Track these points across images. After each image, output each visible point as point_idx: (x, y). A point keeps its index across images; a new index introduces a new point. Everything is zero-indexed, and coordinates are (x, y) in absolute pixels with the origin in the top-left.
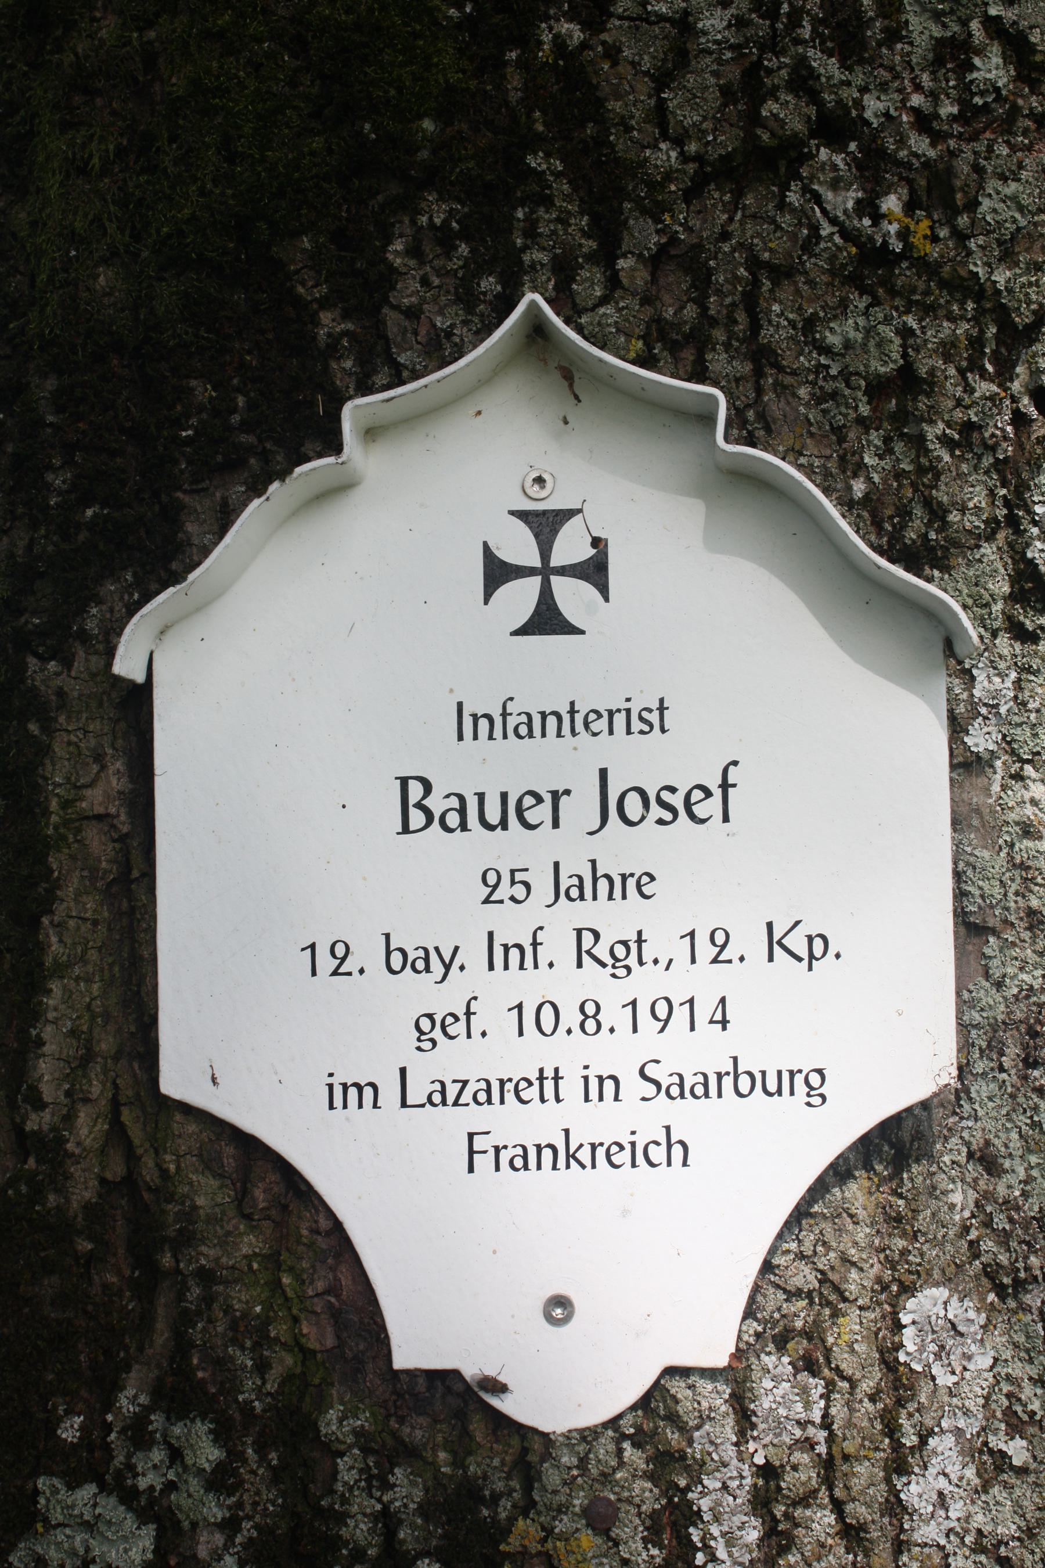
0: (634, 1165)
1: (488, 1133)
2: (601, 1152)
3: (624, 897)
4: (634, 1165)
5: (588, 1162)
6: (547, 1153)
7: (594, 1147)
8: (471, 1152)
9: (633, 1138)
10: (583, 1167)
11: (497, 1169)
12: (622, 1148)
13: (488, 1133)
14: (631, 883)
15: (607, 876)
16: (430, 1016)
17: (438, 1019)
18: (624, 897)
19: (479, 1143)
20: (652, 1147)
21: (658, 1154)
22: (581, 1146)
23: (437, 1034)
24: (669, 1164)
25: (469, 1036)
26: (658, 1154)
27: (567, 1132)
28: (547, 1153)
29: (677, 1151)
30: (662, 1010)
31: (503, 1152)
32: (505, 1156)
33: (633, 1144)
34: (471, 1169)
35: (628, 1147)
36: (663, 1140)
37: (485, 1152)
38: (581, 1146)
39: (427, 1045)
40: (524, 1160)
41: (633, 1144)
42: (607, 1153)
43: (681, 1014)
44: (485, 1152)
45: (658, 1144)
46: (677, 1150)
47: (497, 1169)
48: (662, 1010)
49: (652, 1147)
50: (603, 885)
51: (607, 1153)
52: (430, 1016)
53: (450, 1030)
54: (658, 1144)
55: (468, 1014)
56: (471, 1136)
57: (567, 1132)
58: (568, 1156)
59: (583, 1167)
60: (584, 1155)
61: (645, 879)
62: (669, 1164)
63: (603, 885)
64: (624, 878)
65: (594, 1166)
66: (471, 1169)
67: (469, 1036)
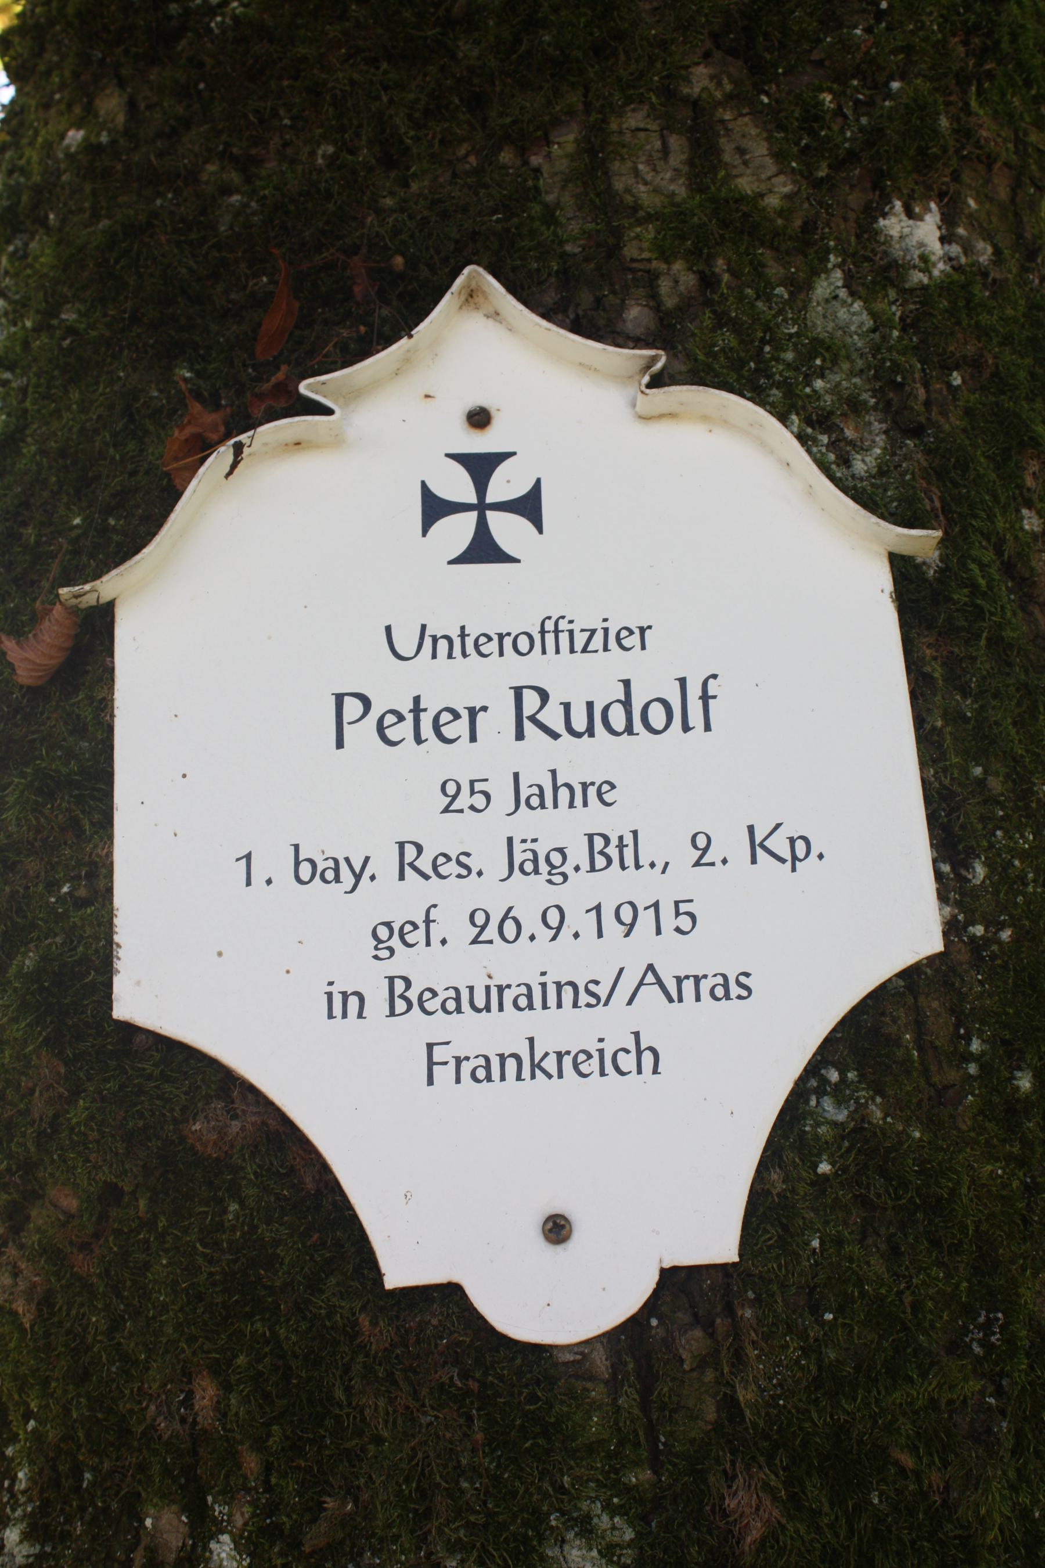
0: (603, 1073)
1: (447, 1043)
2: (567, 1061)
3: (585, 804)
4: (603, 1073)
5: (554, 1071)
6: (511, 1064)
7: (560, 1056)
8: (431, 1063)
9: (600, 1046)
10: (550, 1076)
11: (458, 1080)
12: (589, 1056)
13: (447, 1043)
14: (592, 791)
15: (568, 786)
16: (388, 925)
17: (396, 927)
18: (585, 804)
19: (439, 1054)
20: (621, 1054)
21: (627, 1062)
22: (546, 1054)
23: (395, 942)
24: (639, 1072)
25: (428, 944)
26: (627, 1062)
27: (531, 1040)
28: (511, 1064)
29: (648, 1058)
30: (627, 915)
31: (464, 1063)
32: (466, 1068)
33: (601, 1052)
34: (430, 1081)
35: (596, 1055)
36: (632, 1047)
37: (446, 1063)
38: (546, 1054)
39: (385, 954)
40: (487, 1070)
41: (601, 1052)
42: (575, 1062)
43: (646, 918)
44: (446, 1063)
45: (627, 1051)
46: (648, 1058)
47: (458, 1080)
48: (627, 915)
49: (621, 1054)
50: (564, 794)
51: (575, 1062)
52: (388, 925)
53: (409, 938)
54: (627, 1051)
55: (428, 921)
56: (430, 1047)
57: (531, 1040)
58: (535, 1066)
59: (550, 1076)
60: (550, 1064)
61: (605, 788)
62: (639, 1072)
63: (564, 794)
64: (585, 786)
65: (560, 1076)
66: (430, 1081)
67: (428, 944)
